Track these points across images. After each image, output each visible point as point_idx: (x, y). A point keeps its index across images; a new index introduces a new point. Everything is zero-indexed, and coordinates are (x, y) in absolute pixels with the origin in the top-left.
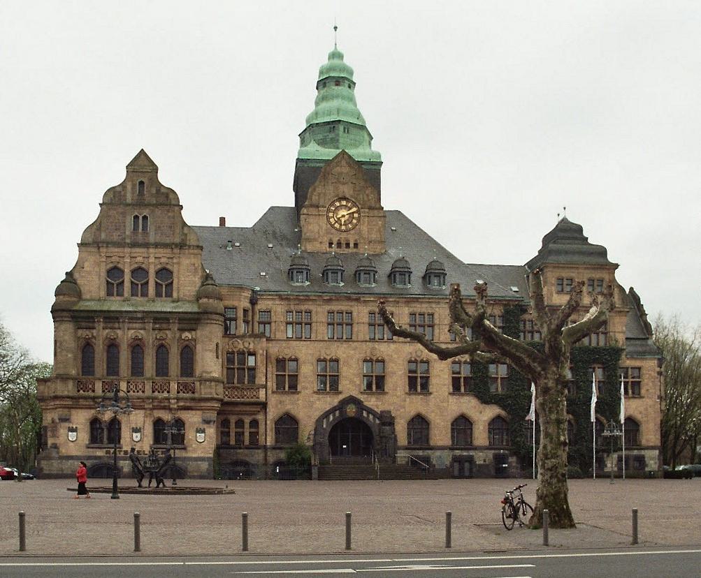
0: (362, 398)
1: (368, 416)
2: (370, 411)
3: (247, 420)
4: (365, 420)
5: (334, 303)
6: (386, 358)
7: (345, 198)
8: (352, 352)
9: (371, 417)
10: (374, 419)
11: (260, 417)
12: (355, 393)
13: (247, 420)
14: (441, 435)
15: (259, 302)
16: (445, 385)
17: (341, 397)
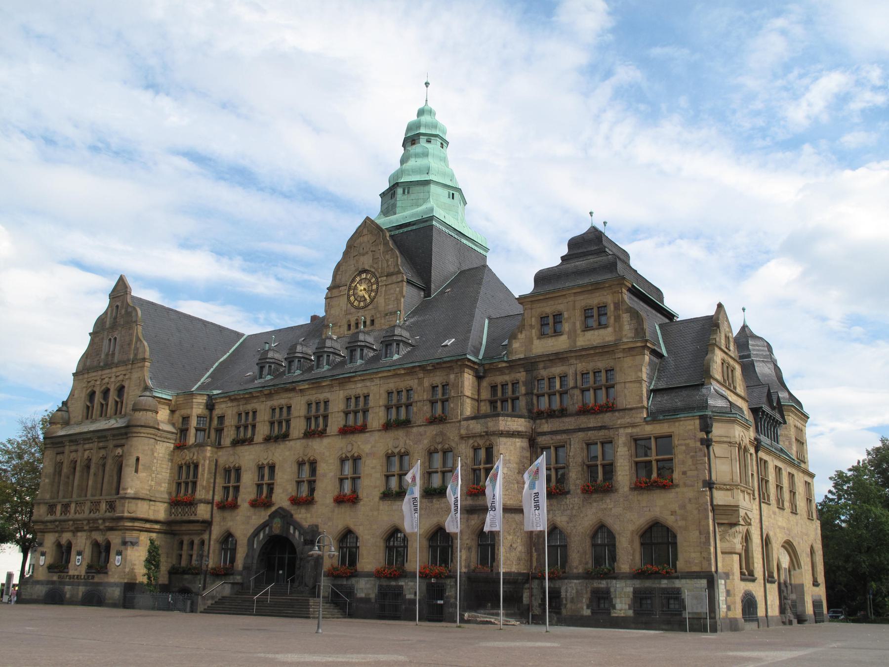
0: (293, 509)
1: (294, 532)
2: (298, 526)
3: (197, 541)
4: (291, 538)
5: (275, 397)
6: (318, 458)
7: (365, 271)
8: (287, 453)
9: (297, 533)
10: (300, 537)
11: (206, 537)
12: (286, 504)
13: (197, 541)
14: (371, 558)
15: (216, 407)
16: (375, 487)
17: (273, 509)
